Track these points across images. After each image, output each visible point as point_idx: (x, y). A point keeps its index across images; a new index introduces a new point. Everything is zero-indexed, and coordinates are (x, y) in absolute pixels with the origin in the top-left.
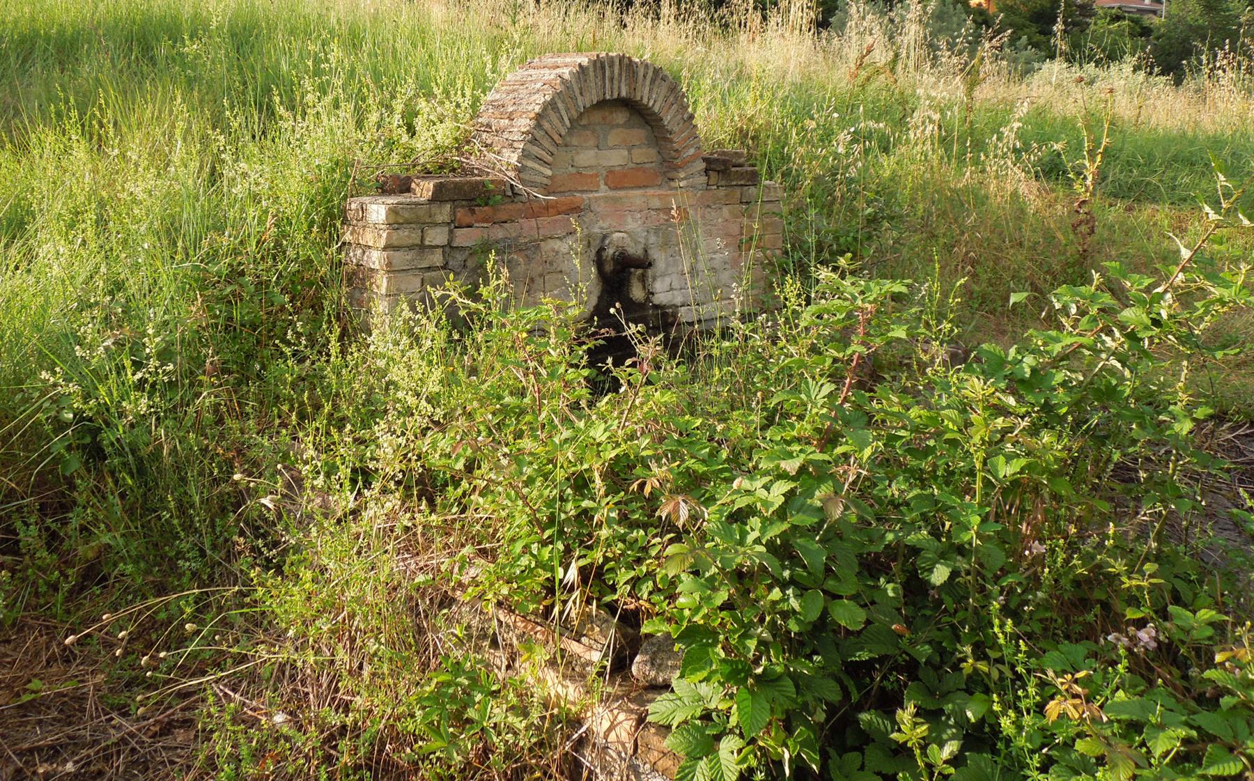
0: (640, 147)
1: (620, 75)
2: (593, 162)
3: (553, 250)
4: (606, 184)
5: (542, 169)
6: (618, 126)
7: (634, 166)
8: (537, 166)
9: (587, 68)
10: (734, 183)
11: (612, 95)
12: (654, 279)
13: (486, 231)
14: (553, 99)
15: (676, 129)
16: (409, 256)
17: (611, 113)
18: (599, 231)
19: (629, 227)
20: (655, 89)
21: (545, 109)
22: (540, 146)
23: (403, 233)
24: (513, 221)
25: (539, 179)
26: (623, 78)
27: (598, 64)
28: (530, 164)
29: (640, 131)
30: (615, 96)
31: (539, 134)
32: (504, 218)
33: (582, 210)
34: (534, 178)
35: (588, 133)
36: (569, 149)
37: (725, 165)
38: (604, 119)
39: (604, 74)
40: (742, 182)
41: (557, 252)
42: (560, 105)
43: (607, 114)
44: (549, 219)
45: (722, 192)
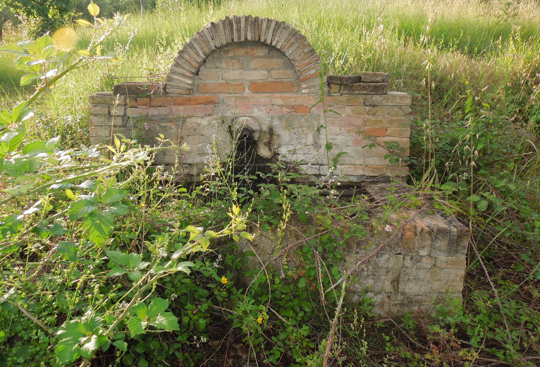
0: (278, 69)
1: (246, 27)
2: (238, 77)
3: (196, 123)
4: (249, 90)
5: (184, 80)
6: (259, 57)
7: (274, 80)
8: (180, 78)
9: (218, 25)
10: (357, 92)
11: (239, 38)
12: (279, 146)
13: (146, 110)
14: (190, 42)
15: (298, 58)
16: (103, 119)
17: (253, 50)
18: (231, 115)
19: (255, 114)
20: (278, 35)
21: (185, 48)
22: (182, 67)
23: (98, 108)
24: (164, 106)
25: (182, 85)
26: (249, 29)
27: (227, 22)
28: (176, 77)
29: (278, 60)
30: (274, 44)
31: (180, 62)
32: (159, 104)
33: (216, 103)
34: (178, 84)
35: (235, 61)
36: (219, 70)
37: (341, 81)
38: (247, 53)
39: (232, 28)
40: (365, 92)
41: (199, 125)
42: (196, 46)
43: (249, 50)
44: (191, 107)
45: (344, 98)
